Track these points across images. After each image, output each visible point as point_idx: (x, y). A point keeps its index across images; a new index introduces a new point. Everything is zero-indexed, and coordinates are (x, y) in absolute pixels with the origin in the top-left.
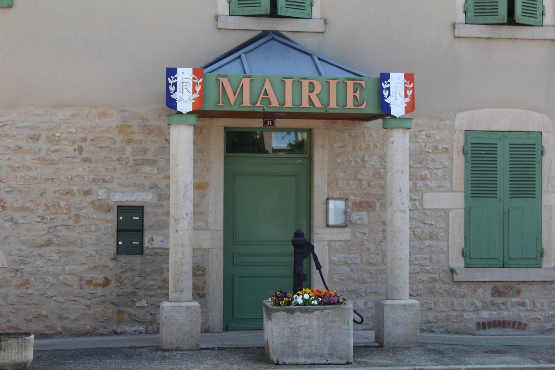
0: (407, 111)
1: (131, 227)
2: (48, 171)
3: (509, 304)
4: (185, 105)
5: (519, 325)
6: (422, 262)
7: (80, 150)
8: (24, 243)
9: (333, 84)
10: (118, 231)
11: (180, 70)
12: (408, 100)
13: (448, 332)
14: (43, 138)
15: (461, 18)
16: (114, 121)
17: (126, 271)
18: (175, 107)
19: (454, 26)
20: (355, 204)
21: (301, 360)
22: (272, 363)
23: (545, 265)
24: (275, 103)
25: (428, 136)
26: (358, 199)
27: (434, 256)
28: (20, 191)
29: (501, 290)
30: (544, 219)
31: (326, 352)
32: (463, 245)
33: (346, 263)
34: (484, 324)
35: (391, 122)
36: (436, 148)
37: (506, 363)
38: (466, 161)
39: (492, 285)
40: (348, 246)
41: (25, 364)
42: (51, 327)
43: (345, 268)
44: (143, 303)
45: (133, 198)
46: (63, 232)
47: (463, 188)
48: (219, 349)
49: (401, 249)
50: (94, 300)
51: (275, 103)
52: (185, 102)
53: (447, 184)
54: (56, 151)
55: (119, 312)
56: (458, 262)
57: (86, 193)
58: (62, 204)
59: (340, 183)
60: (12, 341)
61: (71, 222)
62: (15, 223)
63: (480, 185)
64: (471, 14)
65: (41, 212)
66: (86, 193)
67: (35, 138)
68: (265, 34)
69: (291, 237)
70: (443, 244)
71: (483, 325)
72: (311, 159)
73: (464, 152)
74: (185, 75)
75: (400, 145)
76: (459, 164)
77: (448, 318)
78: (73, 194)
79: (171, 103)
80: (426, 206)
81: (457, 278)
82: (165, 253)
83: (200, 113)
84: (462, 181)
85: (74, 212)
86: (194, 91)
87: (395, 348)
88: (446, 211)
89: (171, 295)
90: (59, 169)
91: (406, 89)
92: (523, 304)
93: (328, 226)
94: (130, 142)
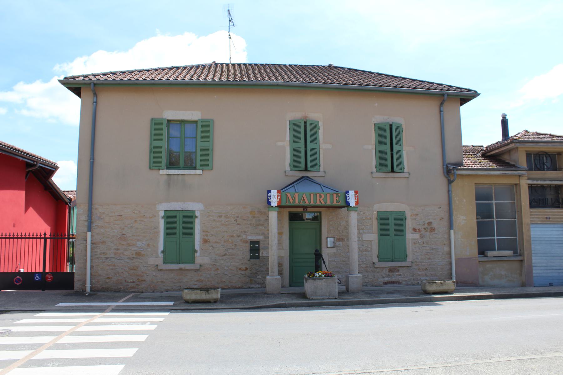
1: (255, 249)
4: (274, 203)
5: (399, 283)
7: (236, 221)
9: (328, 195)
10: (250, 250)
15: (374, 170)
19: (372, 173)
21: (319, 298)
22: (308, 299)
23: (408, 260)
25: (364, 213)
26: (338, 237)
29: (392, 270)
31: (328, 294)
35: (350, 209)
44: (260, 277)
49: (355, 255)
51: (307, 203)
52: (274, 203)
55: (251, 280)
56: (376, 260)
57: (239, 236)
58: (230, 240)
60: (213, 291)
61: (233, 247)
62: (213, 248)
63: (383, 231)
64: (378, 168)
66: (239, 236)
67: (220, 217)
68: (303, 177)
69: (314, 252)
71: (386, 283)
72: (321, 223)
74: (274, 193)
76: (375, 224)
79: (269, 203)
81: (376, 266)
82: (267, 258)
83: (279, 206)
87: (353, 293)
88: (371, 241)
89: (270, 274)
92: (400, 275)
94: (254, 217)
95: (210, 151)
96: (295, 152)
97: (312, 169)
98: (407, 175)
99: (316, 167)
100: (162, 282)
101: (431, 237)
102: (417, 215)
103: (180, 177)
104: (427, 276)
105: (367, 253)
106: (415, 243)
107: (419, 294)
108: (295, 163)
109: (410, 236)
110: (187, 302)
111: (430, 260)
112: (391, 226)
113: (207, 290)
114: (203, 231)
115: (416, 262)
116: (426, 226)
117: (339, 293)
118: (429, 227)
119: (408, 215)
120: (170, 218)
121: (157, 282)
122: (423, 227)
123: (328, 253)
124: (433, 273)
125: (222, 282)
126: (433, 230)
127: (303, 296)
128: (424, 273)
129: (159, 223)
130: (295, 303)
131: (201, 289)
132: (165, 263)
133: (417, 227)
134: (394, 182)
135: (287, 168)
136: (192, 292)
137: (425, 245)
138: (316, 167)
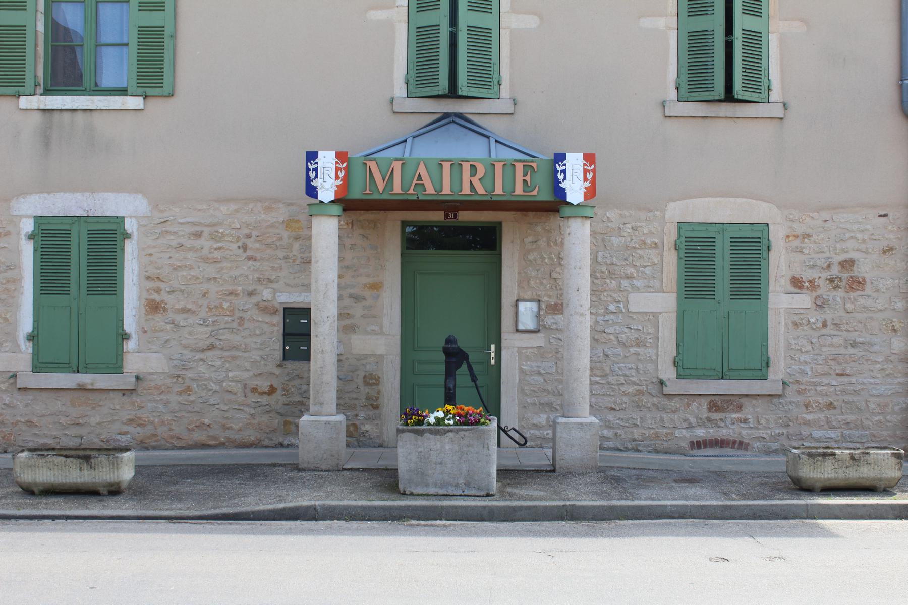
0: (586, 198)
2: (210, 270)
3: (729, 420)
4: (327, 191)
5: (740, 445)
6: (627, 372)
7: (245, 248)
8: (185, 347)
9: (499, 167)
10: (285, 335)
11: (320, 153)
12: (587, 184)
13: (657, 452)
14: (205, 235)
15: (673, 95)
16: (281, 214)
17: (293, 378)
18: (316, 196)
19: (663, 104)
20: (549, 306)
21: (432, 490)
22: (399, 492)
23: (771, 376)
24: (430, 189)
26: (552, 301)
27: (640, 366)
28: (182, 291)
29: (718, 404)
30: (771, 324)
31: (461, 481)
32: (675, 354)
33: (539, 373)
34: (698, 443)
35: (566, 211)
36: (644, 243)
37: (686, 498)
38: (679, 258)
39: (709, 399)
40: (541, 353)
41: (118, 484)
42: (214, 438)
43: (536, 378)
45: (300, 299)
46: (226, 336)
47: (675, 288)
48: (364, 470)
49: (581, 358)
50: (259, 409)
51: (430, 189)
52: (327, 191)
53: (657, 284)
54: (220, 248)
55: (286, 423)
56: (668, 373)
57: (251, 294)
58: (225, 305)
59: (532, 282)
60: (103, 458)
61: (235, 325)
62: (177, 326)
64: (684, 90)
65: (203, 314)
66: (251, 294)
67: (198, 235)
68: (446, 116)
69: (443, 344)
70: (651, 352)
71: (698, 445)
72: (501, 255)
73: (677, 248)
74: (327, 160)
75: (578, 236)
76: (670, 262)
77: (657, 436)
78: (237, 295)
79: (312, 191)
80: (631, 309)
81: (666, 390)
83: (347, 205)
84: (674, 280)
85: (237, 314)
86: (337, 177)
87: (569, 474)
88: (656, 315)
89: (313, 409)
90: (222, 268)
91: (586, 171)
92: (745, 421)
93: (517, 331)
94: (297, 238)
95: (167, 42)
96: (422, 40)
97: (473, 92)
98: (778, 112)
99: (488, 87)
100: (30, 423)
101: (849, 306)
102: (809, 236)
103: (79, 116)
104: (833, 428)
105: (641, 350)
106: (795, 324)
107: (777, 489)
108: (421, 76)
109: (781, 301)
110: (29, 491)
111: (846, 379)
112: (722, 269)
113: (84, 455)
114: (148, 278)
115: (798, 382)
116: (835, 271)
117: (503, 473)
118: (845, 276)
119: (777, 235)
120: (51, 238)
121: (16, 424)
122: (826, 275)
123: (520, 348)
124: (851, 418)
125: (200, 426)
126: (856, 284)
127: (388, 480)
128: (822, 416)
129: (19, 252)
130: (346, 508)
131: (65, 452)
132: (38, 367)
133: (807, 275)
134: (733, 135)
135: (400, 90)
136: (42, 461)
137: (829, 330)
138: (488, 87)
